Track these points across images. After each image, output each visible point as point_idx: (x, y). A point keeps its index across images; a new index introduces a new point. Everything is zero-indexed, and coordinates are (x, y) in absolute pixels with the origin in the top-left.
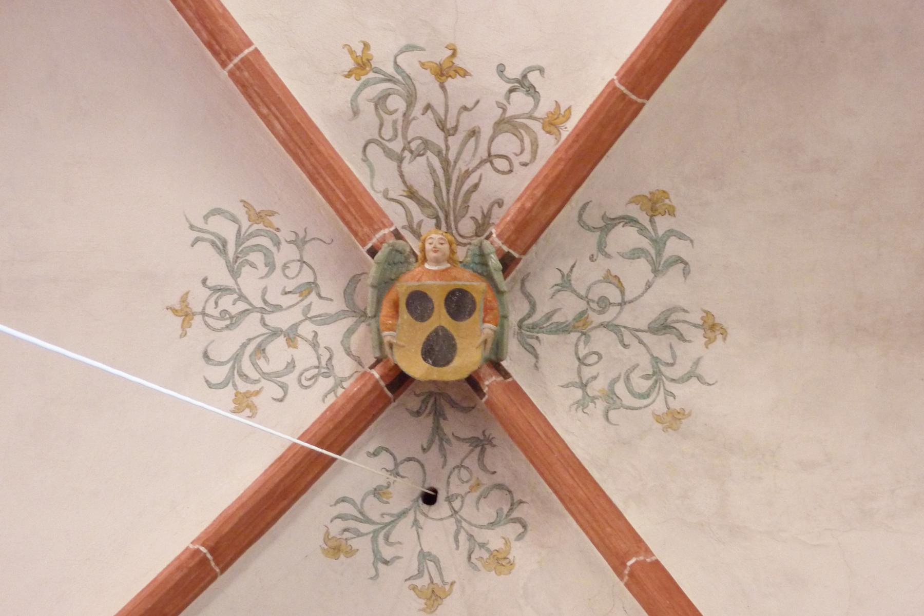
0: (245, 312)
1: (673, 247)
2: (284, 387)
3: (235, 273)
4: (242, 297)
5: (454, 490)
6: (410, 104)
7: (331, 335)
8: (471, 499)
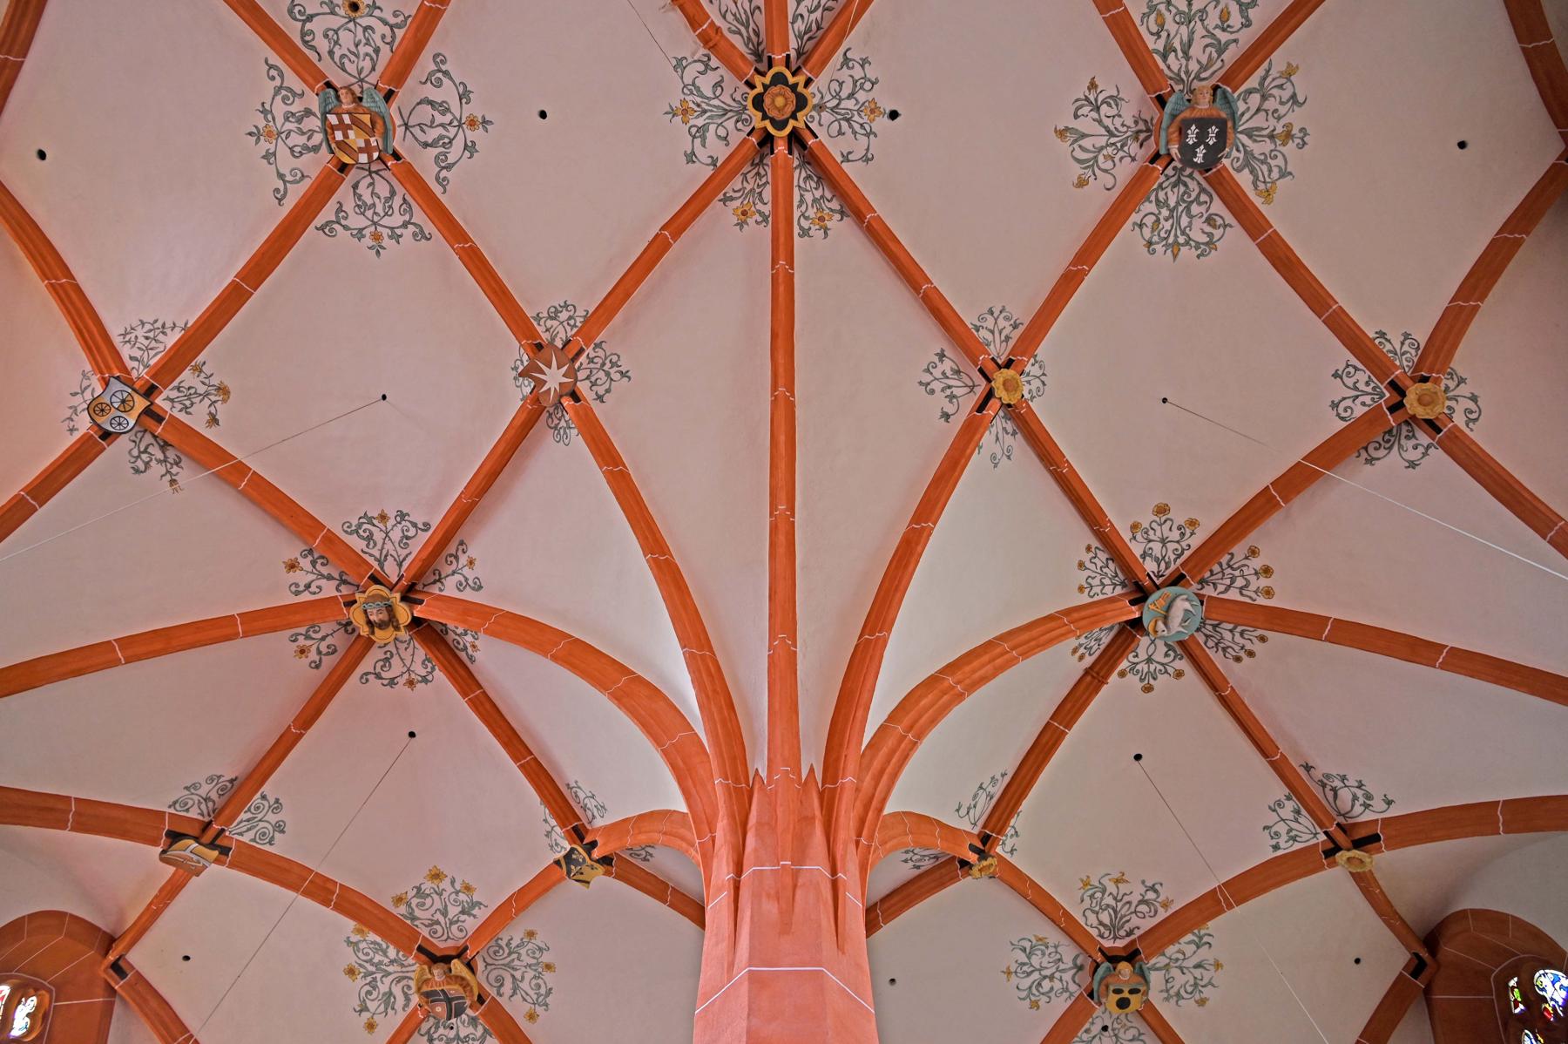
0: (1032, 971)
1: (1206, 939)
2: (1050, 997)
3: (1029, 958)
4: (1032, 966)
5: (1116, 1026)
6: (1103, 895)
7: (1067, 976)
8: (1122, 1031)
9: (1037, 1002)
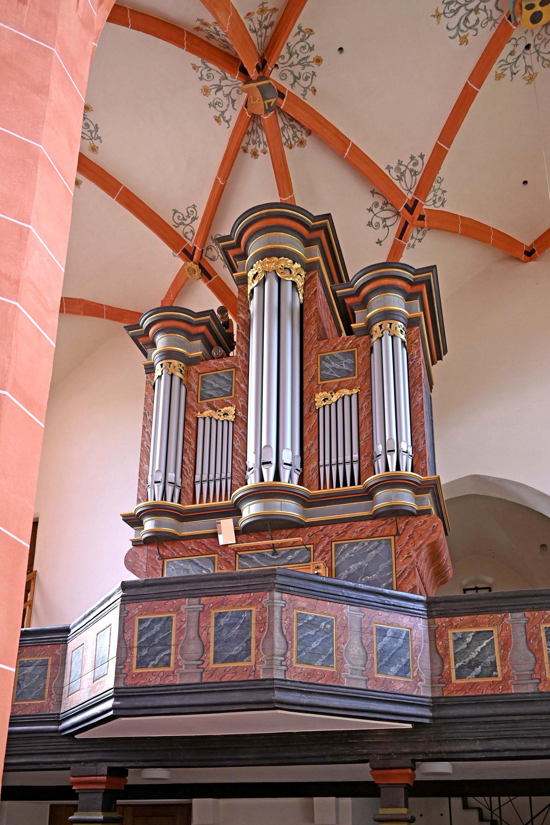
2: (476, 30)
4: (457, 3)
9: (465, 37)
